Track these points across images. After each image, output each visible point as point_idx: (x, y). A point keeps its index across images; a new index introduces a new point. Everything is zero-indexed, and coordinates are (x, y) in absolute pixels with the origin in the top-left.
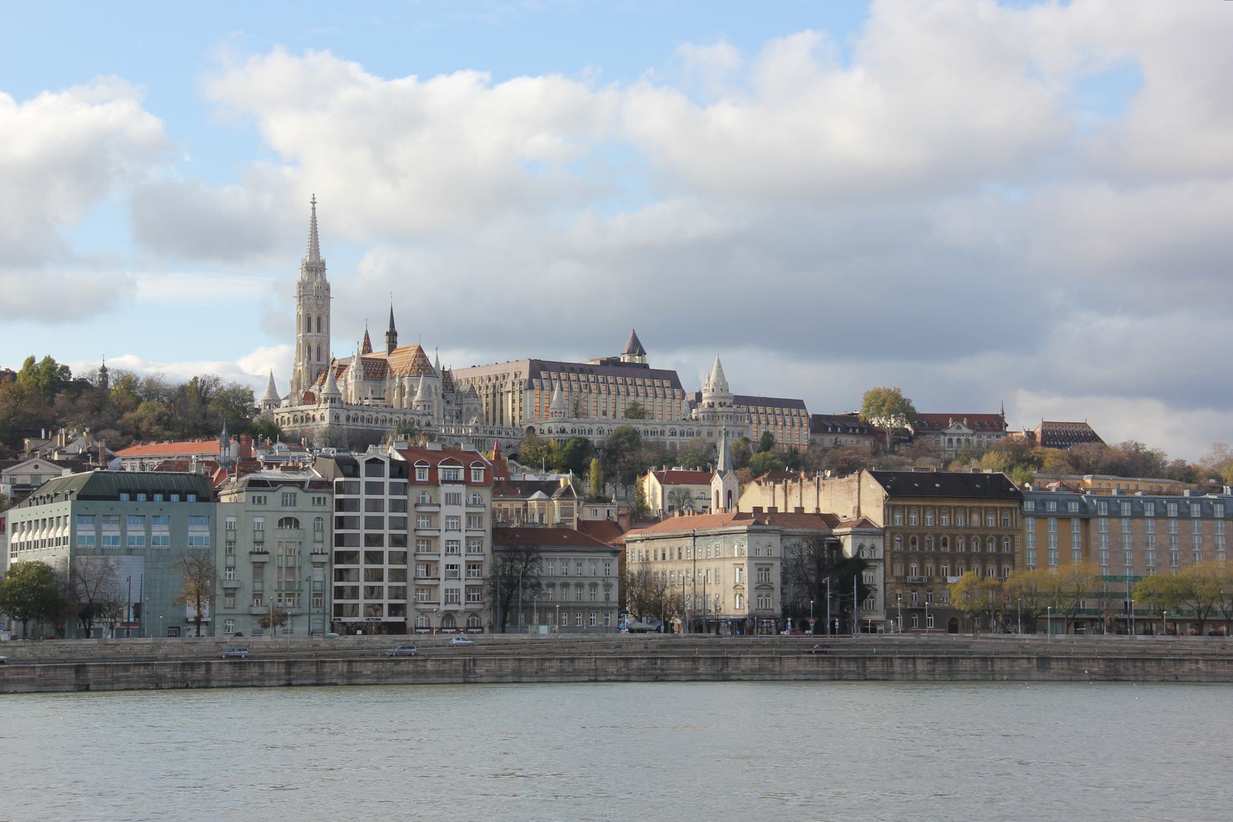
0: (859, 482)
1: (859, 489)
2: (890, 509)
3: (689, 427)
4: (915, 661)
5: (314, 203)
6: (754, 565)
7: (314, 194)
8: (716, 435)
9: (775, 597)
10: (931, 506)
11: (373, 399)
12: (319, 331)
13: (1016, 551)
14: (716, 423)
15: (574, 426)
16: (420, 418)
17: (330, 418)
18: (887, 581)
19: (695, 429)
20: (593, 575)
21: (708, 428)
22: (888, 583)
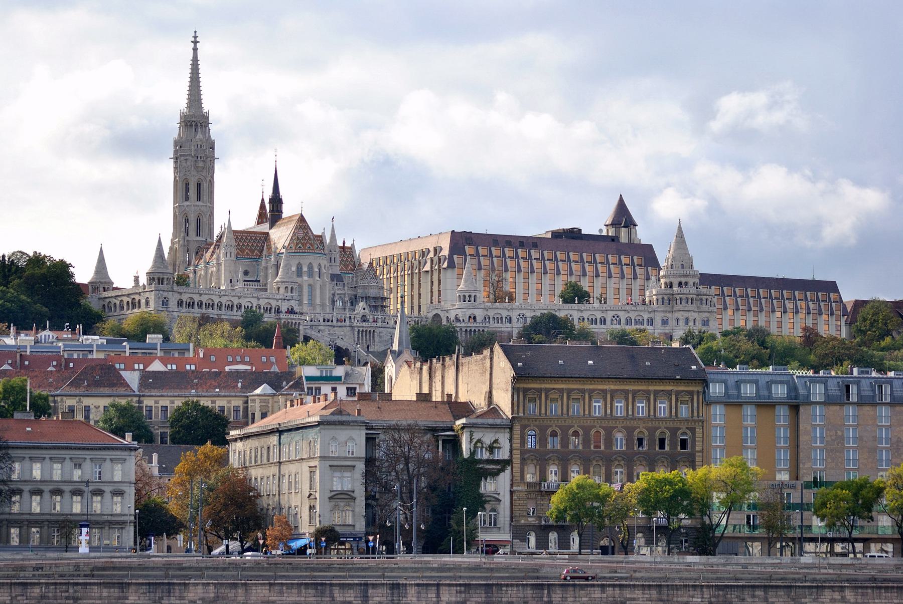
0: (491, 359)
1: (491, 368)
2: (521, 394)
3: (637, 313)
4: (438, 590)
5: (195, 42)
6: (329, 468)
7: (195, 32)
8: (672, 323)
9: (357, 510)
10: (578, 389)
11: (245, 281)
12: (199, 198)
13: (697, 448)
14: (673, 306)
15: (486, 313)
16: (279, 303)
17: (156, 302)
18: (515, 488)
19: (646, 316)
20: (98, 480)
21: (662, 314)
22: (515, 491)
